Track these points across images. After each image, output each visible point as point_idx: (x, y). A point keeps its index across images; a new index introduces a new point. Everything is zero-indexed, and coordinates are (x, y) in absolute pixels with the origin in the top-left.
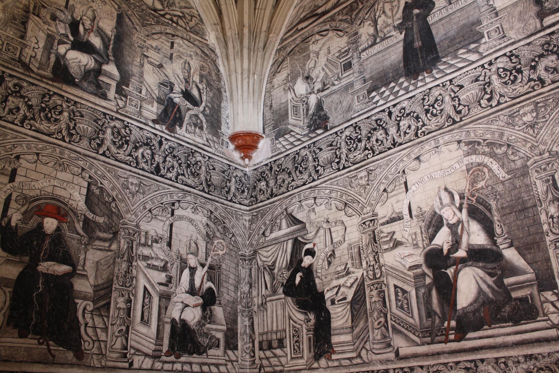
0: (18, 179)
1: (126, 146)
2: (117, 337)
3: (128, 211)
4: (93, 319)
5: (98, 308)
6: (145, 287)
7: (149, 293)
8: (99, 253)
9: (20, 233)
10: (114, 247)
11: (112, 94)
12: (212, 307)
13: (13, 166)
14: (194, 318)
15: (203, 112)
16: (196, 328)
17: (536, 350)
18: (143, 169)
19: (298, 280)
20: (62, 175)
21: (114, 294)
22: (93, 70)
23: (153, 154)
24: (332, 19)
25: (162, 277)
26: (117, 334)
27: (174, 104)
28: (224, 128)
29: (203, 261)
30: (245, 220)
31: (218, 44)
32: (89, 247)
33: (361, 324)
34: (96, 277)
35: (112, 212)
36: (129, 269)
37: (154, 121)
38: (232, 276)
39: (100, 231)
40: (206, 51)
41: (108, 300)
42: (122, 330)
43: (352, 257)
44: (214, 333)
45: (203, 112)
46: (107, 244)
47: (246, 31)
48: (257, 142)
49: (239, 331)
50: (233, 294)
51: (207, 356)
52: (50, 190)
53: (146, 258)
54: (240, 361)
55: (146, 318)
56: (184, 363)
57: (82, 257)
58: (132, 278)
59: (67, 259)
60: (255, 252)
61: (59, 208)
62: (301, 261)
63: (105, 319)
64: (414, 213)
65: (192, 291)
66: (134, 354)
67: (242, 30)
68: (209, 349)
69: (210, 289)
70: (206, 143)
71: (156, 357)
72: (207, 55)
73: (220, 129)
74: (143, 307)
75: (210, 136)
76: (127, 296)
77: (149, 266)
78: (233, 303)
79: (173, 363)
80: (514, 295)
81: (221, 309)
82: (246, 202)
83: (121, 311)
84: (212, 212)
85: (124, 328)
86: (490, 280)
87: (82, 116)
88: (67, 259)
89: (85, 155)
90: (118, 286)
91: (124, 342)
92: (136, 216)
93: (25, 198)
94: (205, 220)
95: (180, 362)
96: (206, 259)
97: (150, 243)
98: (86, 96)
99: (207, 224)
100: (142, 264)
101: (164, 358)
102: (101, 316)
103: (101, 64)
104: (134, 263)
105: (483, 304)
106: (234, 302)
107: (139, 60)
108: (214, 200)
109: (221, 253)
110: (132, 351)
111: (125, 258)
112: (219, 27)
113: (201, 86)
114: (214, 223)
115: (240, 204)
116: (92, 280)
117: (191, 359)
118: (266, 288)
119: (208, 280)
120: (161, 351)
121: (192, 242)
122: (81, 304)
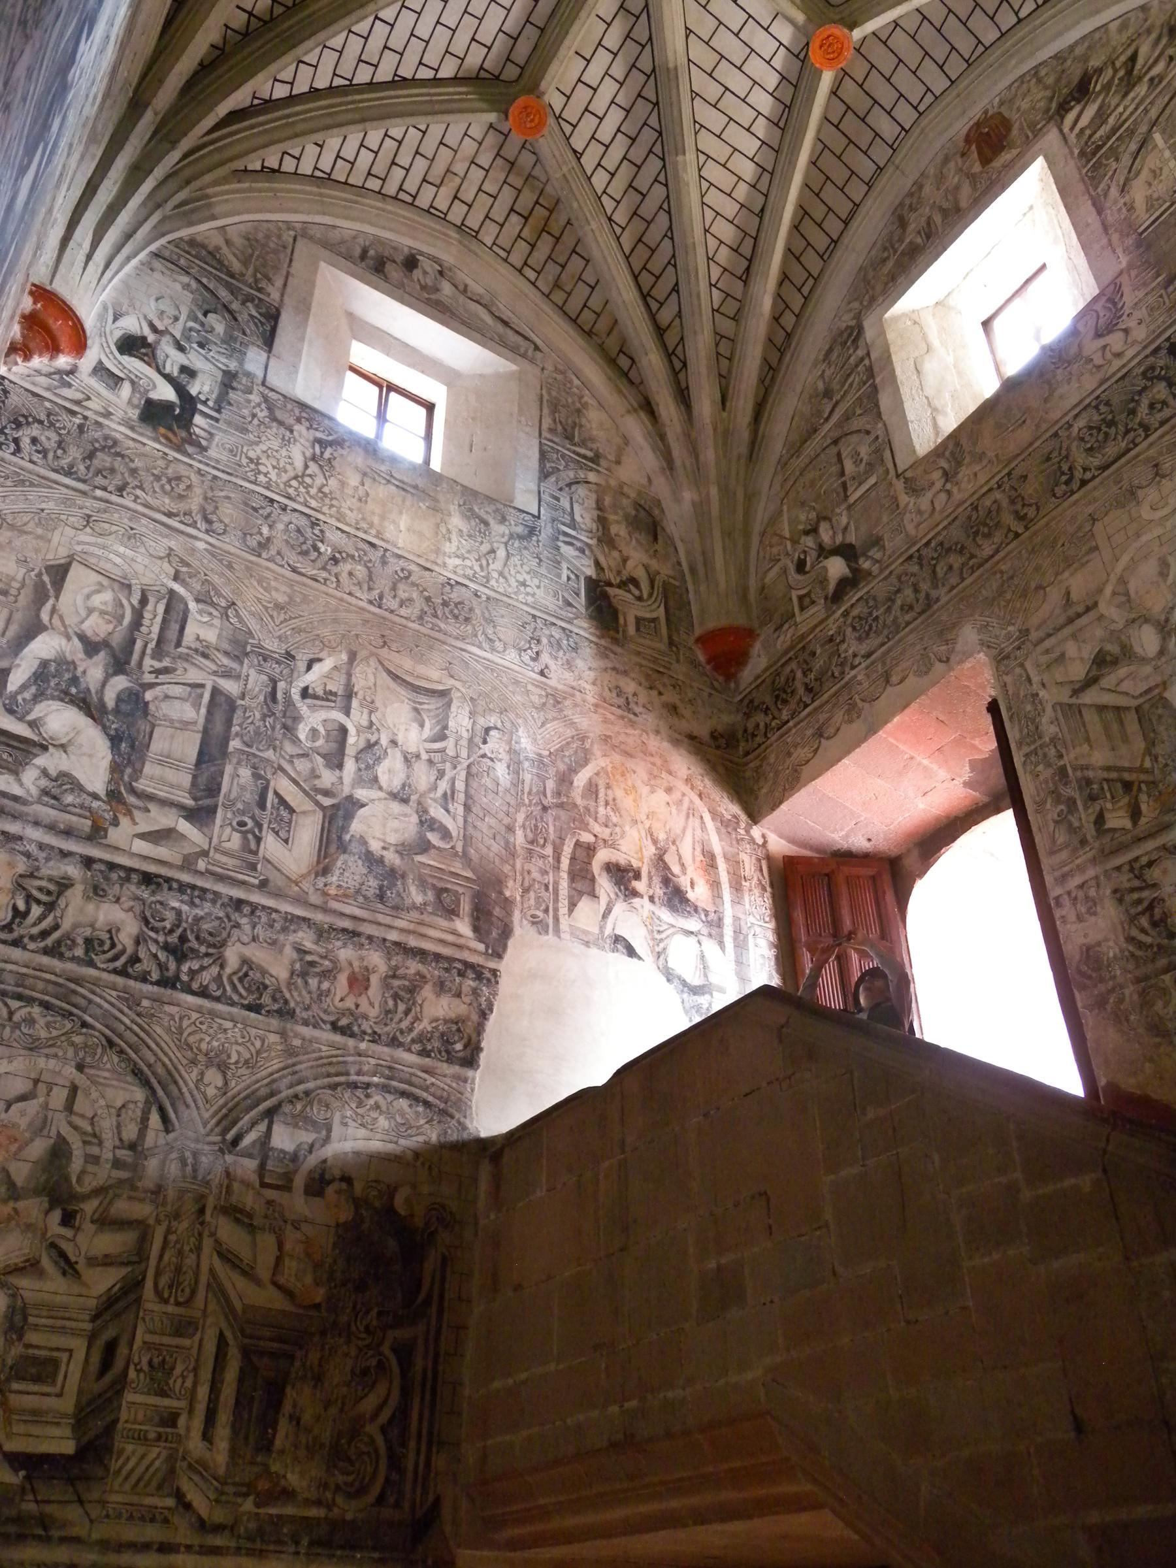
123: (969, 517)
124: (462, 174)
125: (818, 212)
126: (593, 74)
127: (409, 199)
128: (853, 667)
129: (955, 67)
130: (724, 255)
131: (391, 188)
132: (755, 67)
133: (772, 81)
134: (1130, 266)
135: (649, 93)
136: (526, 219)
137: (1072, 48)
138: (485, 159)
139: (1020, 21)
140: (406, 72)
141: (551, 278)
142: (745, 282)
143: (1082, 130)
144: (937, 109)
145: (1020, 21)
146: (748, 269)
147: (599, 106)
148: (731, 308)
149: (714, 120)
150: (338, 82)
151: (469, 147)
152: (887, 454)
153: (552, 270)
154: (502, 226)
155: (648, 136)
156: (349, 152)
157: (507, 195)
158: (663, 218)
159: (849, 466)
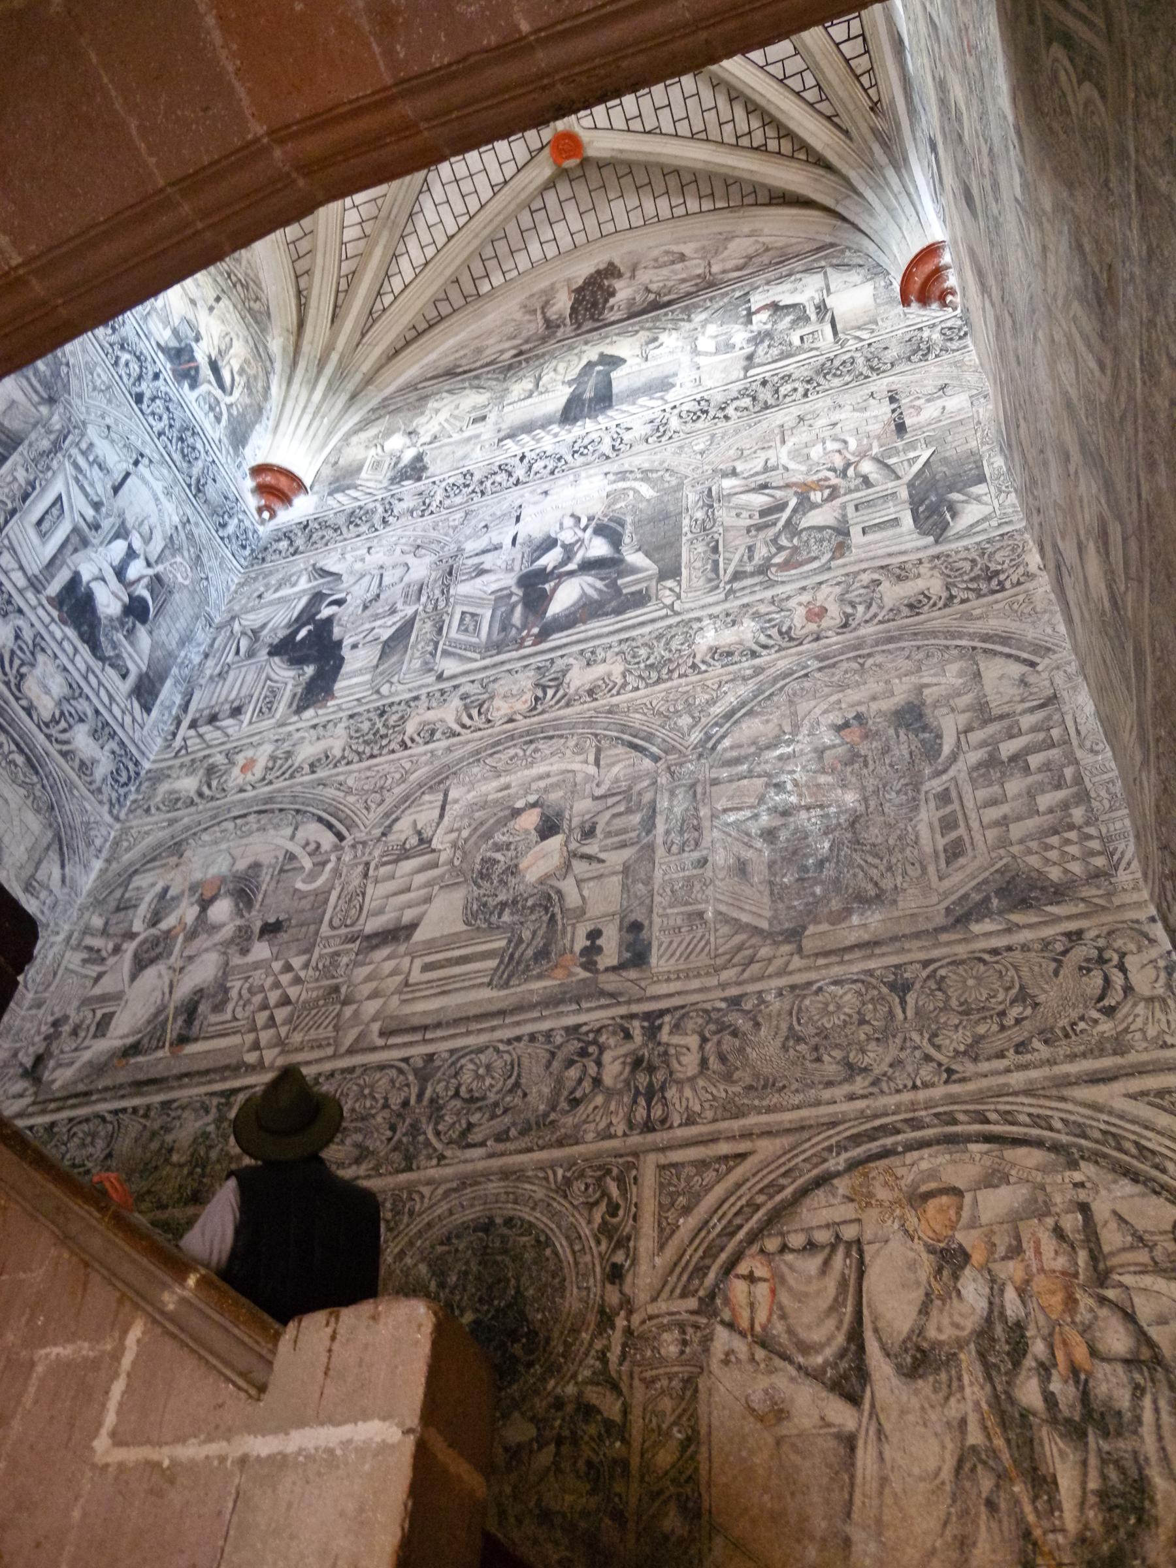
6: (59, 498)
10: (44, 410)
12: (138, 625)
14: (108, 606)
15: (229, 406)
16: (104, 621)
17: (634, 633)
19: (303, 633)
23: (140, 378)
24: (477, 377)
27: (192, 359)
28: (248, 451)
29: (153, 558)
33: (394, 659)
37: (158, 345)
43: (407, 596)
44: (125, 655)
46: (36, 398)
47: (335, 357)
49: (161, 697)
54: (145, 732)
55: (45, 526)
56: (65, 637)
58: (49, 468)
60: (233, 618)
62: (319, 612)
64: (519, 540)
65: (120, 573)
67: (328, 355)
69: (142, 600)
71: (36, 585)
74: (47, 512)
75: (225, 440)
76: (32, 477)
77: (77, 480)
79: (53, 620)
80: (625, 591)
83: (15, 486)
85: (10, 506)
86: (600, 584)
94: (176, 519)
97: (91, 458)
101: (45, 602)
105: (585, 605)
111: (52, 437)
113: (237, 378)
118: (237, 652)
119: (147, 587)
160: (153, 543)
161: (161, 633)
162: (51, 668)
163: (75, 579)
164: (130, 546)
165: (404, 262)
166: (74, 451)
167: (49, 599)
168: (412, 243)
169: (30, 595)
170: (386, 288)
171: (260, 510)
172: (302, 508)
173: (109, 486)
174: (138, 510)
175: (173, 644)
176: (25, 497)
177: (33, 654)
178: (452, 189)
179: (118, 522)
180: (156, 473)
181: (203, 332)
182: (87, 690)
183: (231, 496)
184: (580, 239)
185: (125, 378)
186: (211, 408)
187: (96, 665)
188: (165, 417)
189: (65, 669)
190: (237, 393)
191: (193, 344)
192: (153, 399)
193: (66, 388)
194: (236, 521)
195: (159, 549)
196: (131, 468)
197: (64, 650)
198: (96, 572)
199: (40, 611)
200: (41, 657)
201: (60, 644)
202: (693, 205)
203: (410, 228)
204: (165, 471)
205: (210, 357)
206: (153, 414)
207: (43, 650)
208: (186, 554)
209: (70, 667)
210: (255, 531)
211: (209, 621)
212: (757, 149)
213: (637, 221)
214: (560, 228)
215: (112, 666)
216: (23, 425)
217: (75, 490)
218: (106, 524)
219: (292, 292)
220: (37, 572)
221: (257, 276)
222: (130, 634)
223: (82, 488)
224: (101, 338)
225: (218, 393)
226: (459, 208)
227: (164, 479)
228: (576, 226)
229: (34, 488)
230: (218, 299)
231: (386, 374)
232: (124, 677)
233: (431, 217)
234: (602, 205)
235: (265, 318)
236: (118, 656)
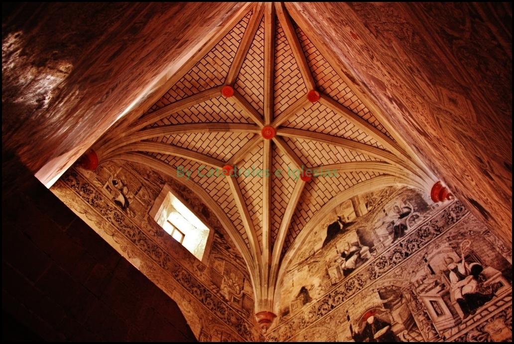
0: (351, 318)
1: (386, 264)
2: (428, 333)
3: (402, 283)
4: (410, 336)
5: (411, 330)
7: (433, 301)
8: (398, 310)
9: (361, 333)
10: (404, 301)
11: (369, 255)
12: (482, 272)
13: (347, 315)
14: (472, 287)
15: (415, 211)
16: (478, 291)
18: (399, 262)
20: (365, 301)
21: (415, 319)
22: (358, 258)
23: (401, 253)
25: (438, 288)
26: (427, 332)
29: (459, 259)
30: (472, 218)
31: (402, 183)
32: (392, 312)
34: (402, 319)
35: (395, 290)
36: (416, 302)
37: (393, 242)
38: (484, 248)
39: (393, 302)
40: (400, 192)
41: (414, 323)
42: (429, 328)
44: (493, 282)
45: (415, 211)
46: (400, 303)
48: (441, 186)
50: (493, 254)
51: (497, 296)
52: (364, 309)
53: (422, 291)
55: (440, 313)
56: (480, 313)
57: (391, 318)
58: (421, 304)
59: (385, 324)
61: (371, 311)
63: (417, 331)
65: (461, 277)
66: (443, 332)
68: (495, 292)
69: (474, 267)
70: (424, 219)
71: (458, 324)
72: (402, 193)
73: (428, 205)
74: (435, 309)
75: (425, 214)
76: (423, 313)
77: (427, 292)
78: (497, 257)
79: (473, 318)
81: (489, 267)
82: (466, 211)
83: (424, 321)
84: (448, 238)
85: (430, 326)
87: (362, 275)
88: (385, 324)
89: (371, 285)
90: (415, 313)
91: (434, 332)
92: (407, 280)
93: (357, 320)
94: (447, 244)
95: (477, 314)
96: (460, 257)
97: (421, 283)
98: (360, 268)
99: (450, 244)
100: (422, 294)
102: (414, 331)
103: (359, 253)
104: (418, 298)
106: (498, 257)
107: (373, 233)
108: (446, 232)
109: (468, 246)
110: (441, 332)
111: (412, 300)
112: (397, 179)
113: (407, 205)
114: (454, 239)
115: (463, 215)
116: (401, 322)
117: (484, 307)
120: (460, 319)
121: (446, 260)
122: (400, 335)
123: (155, 246)
124: (214, 66)
125: (184, 164)
126: (229, 107)
127: (212, 51)
128: (107, 218)
129: (216, 198)
130: (178, 138)
131: (218, 47)
132: (222, 148)
133: (218, 152)
134: (208, 268)
135: (222, 121)
136: (197, 81)
137: (223, 229)
138: (215, 73)
139: (226, 214)
140: (247, 61)
141: (180, 86)
142: (171, 144)
143: (217, 240)
144: (206, 194)
145: (226, 214)
146: (173, 145)
147: (222, 107)
148: (165, 140)
149: (211, 137)
150: (253, 45)
151: (220, 70)
152: (150, 207)
153: (182, 86)
154: (197, 74)
155: (211, 119)
156: (233, 40)
157: (204, 77)
158: (190, 121)
159: (141, 192)
160: (454, 258)
161: (488, 260)
162: (491, 325)
163: (459, 301)
164: (453, 270)
165: (366, 140)
166: (418, 290)
167: (464, 318)
168: (360, 138)
169: (462, 327)
170: (375, 145)
171: (449, 199)
172: (443, 184)
173: (431, 276)
174: (441, 263)
175: (492, 254)
176: (428, 318)
177: (484, 333)
178: (341, 127)
179: (444, 275)
180: (430, 252)
181: (392, 220)
182: (503, 308)
183: (443, 214)
184: (341, 81)
185: (400, 260)
186: (414, 220)
187: (495, 300)
188: (414, 243)
189: (493, 317)
190: (411, 207)
191: (395, 225)
192: (408, 248)
193: (399, 288)
194: (452, 212)
195: (456, 255)
196: (427, 264)
197: (485, 316)
198: (459, 290)
199: (468, 323)
200: (486, 329)
201: (483, 317)
202: (314, 49)
203: (355, 139)
204: (431, 246)
205: (399, 218)
206: (412, 249)
207: (483, 327)
208: (460, 241)
209: (492, 315)
210: (456, 203)
211: (487, 232)
212: (286, 38)
213: (327, 65)
214: (340, 88)
215: (496, 291)
216: (407, 312)
217: (430, 293)
218: (443, 281)
219: (384, 178)
220: (454, 321)
221: (380, 191)
222: (486, 277)
223: (430, 289)
224: (387, 268)
225: (410, 215)
226: (345, 124)
227: (432, 248)
228: (337, 84)
229: (426, 313)
230: (384, 211)
231: (399, 143)
232: (501, 285)
233: (350, 133)
234: (326, 78)
235: (392, 189)
236: (493, 285)
